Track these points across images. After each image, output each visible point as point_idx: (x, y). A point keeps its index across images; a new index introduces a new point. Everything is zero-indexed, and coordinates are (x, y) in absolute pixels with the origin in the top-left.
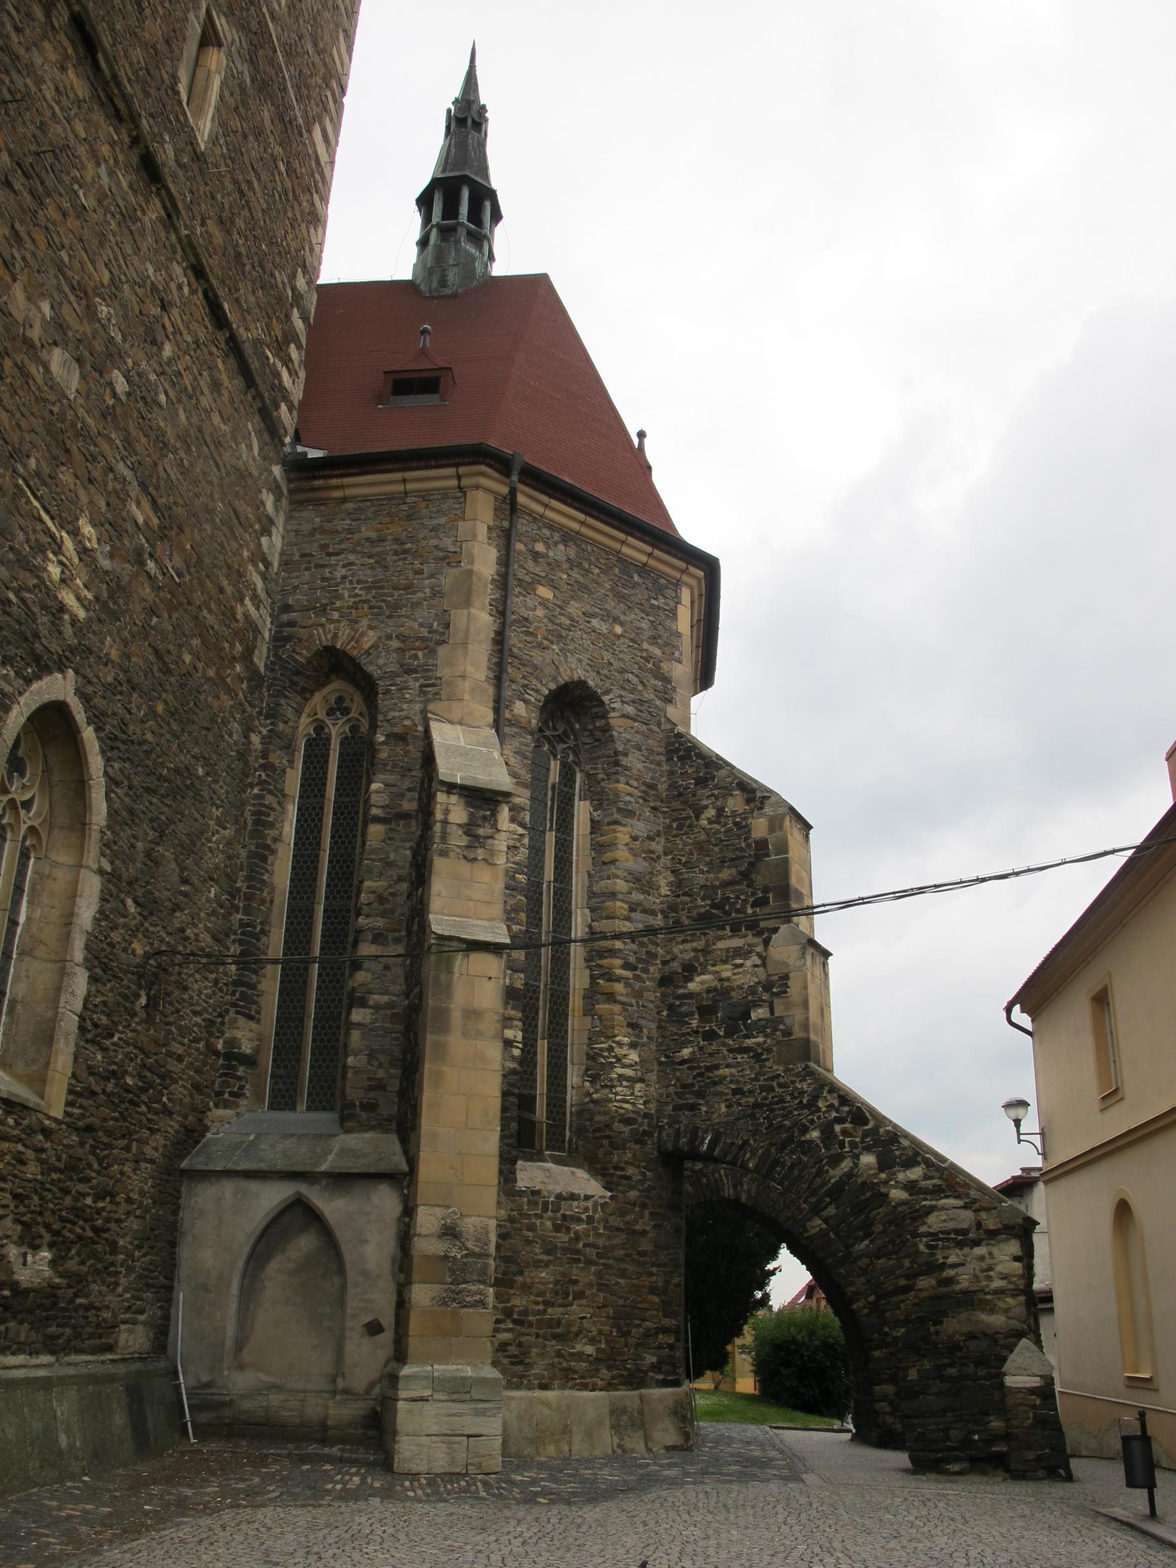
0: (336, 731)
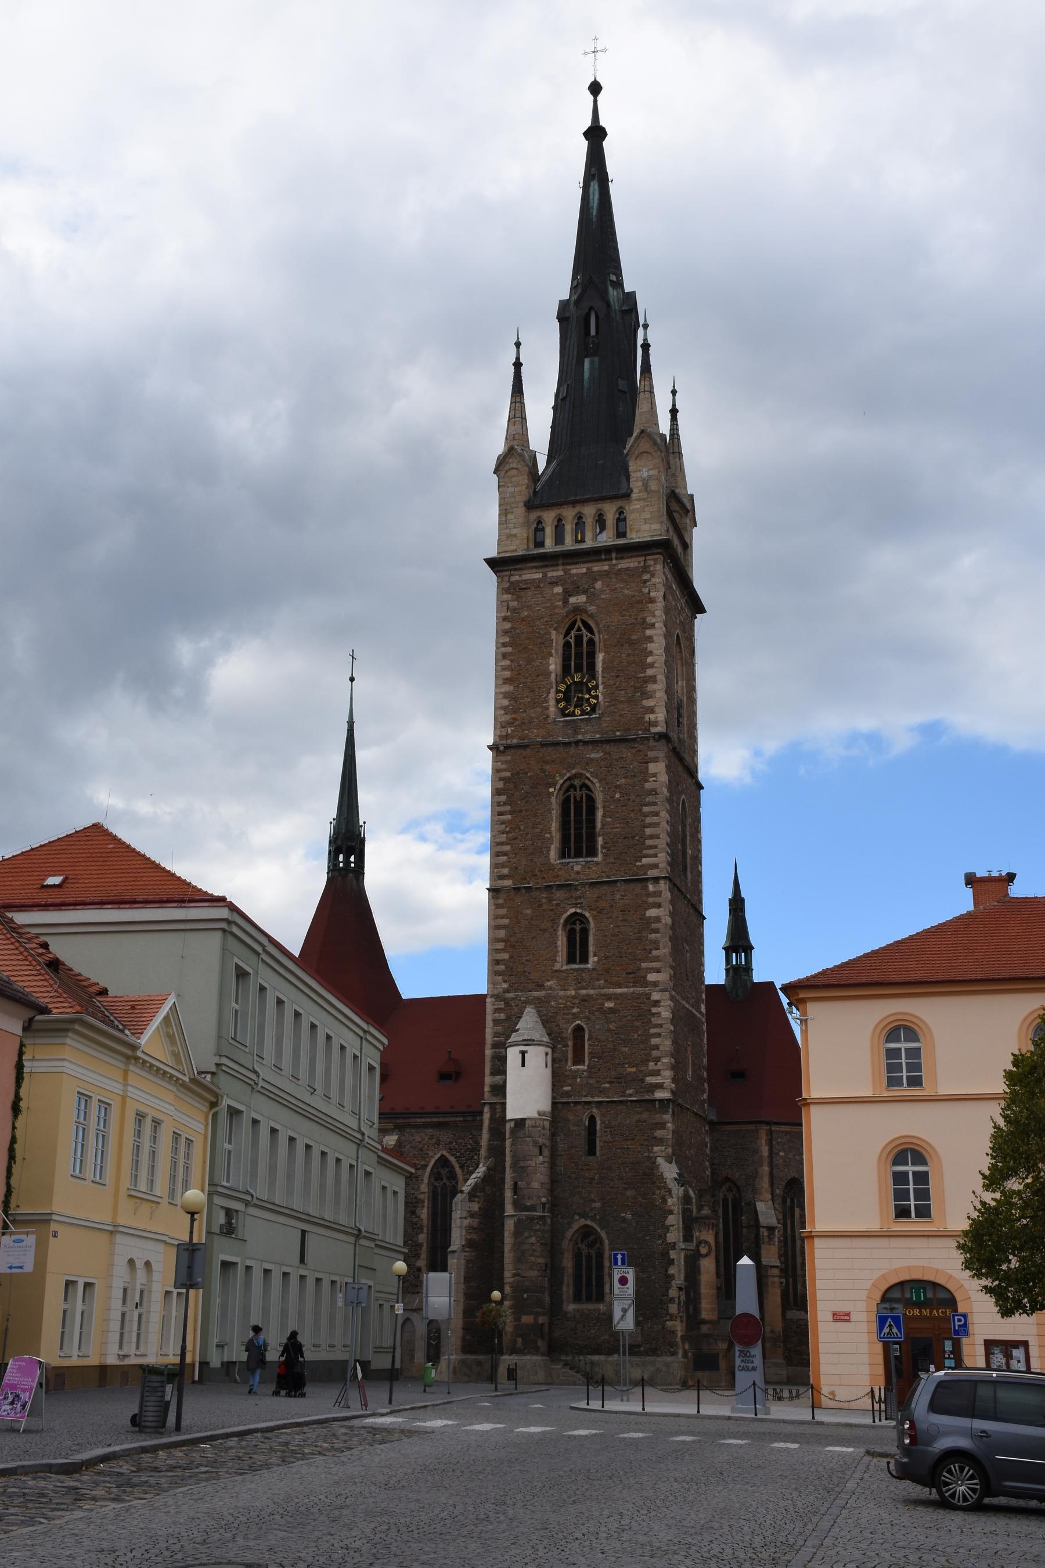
0: (730, 1197)
